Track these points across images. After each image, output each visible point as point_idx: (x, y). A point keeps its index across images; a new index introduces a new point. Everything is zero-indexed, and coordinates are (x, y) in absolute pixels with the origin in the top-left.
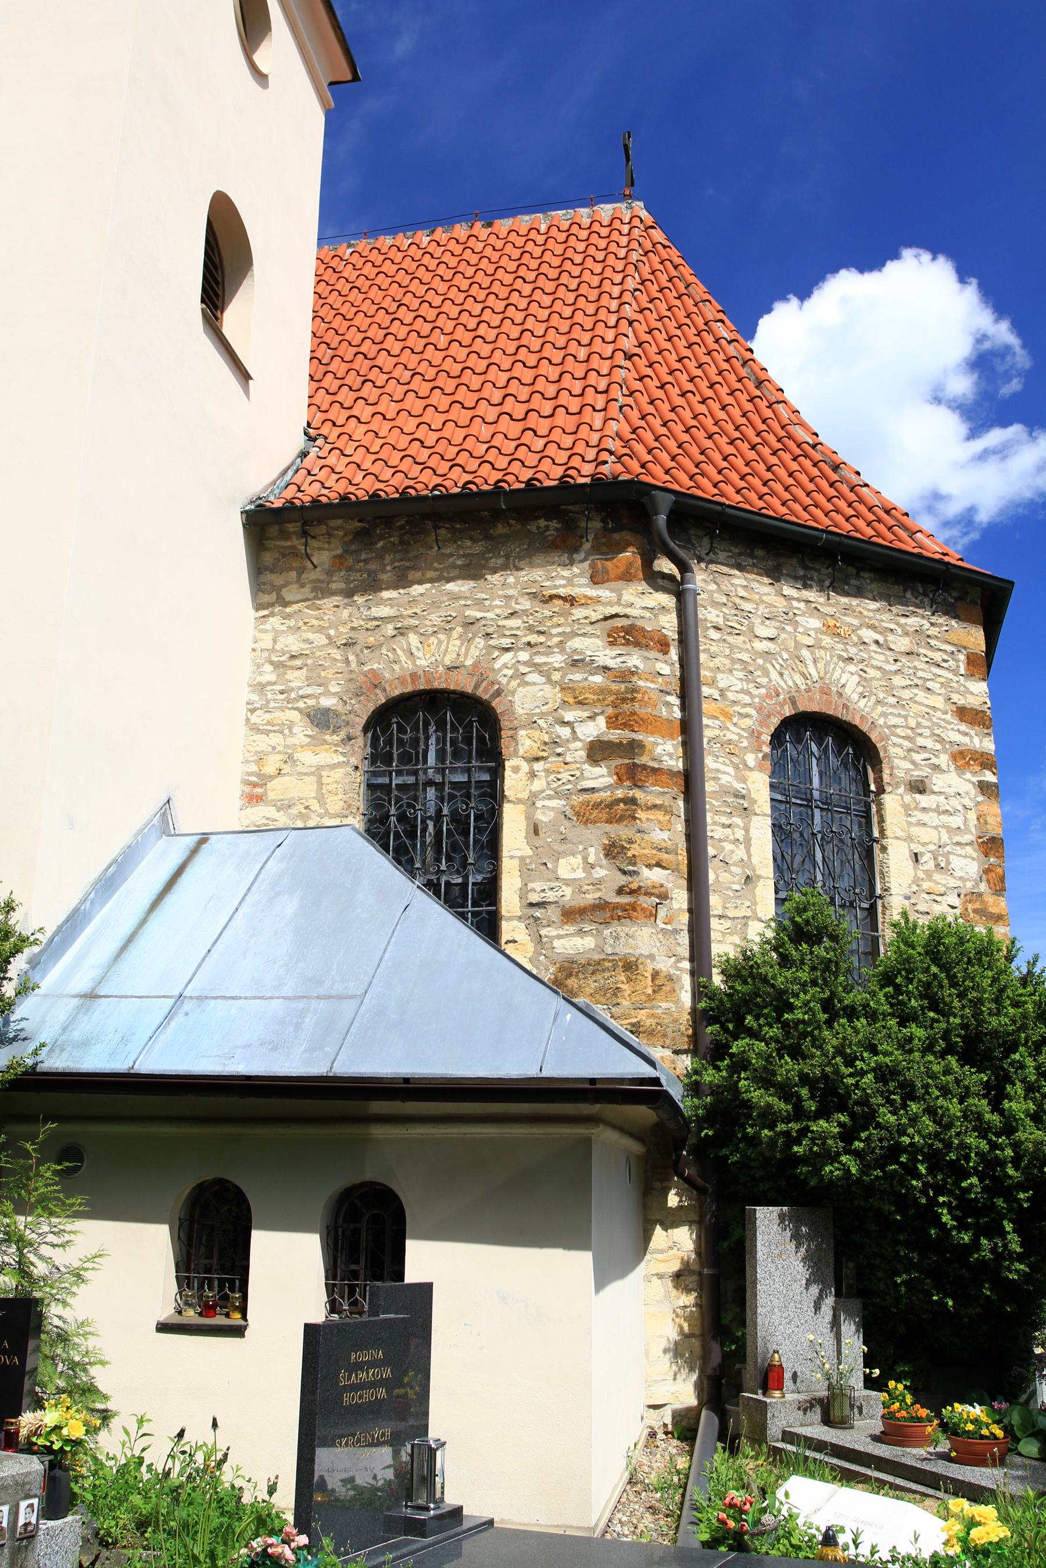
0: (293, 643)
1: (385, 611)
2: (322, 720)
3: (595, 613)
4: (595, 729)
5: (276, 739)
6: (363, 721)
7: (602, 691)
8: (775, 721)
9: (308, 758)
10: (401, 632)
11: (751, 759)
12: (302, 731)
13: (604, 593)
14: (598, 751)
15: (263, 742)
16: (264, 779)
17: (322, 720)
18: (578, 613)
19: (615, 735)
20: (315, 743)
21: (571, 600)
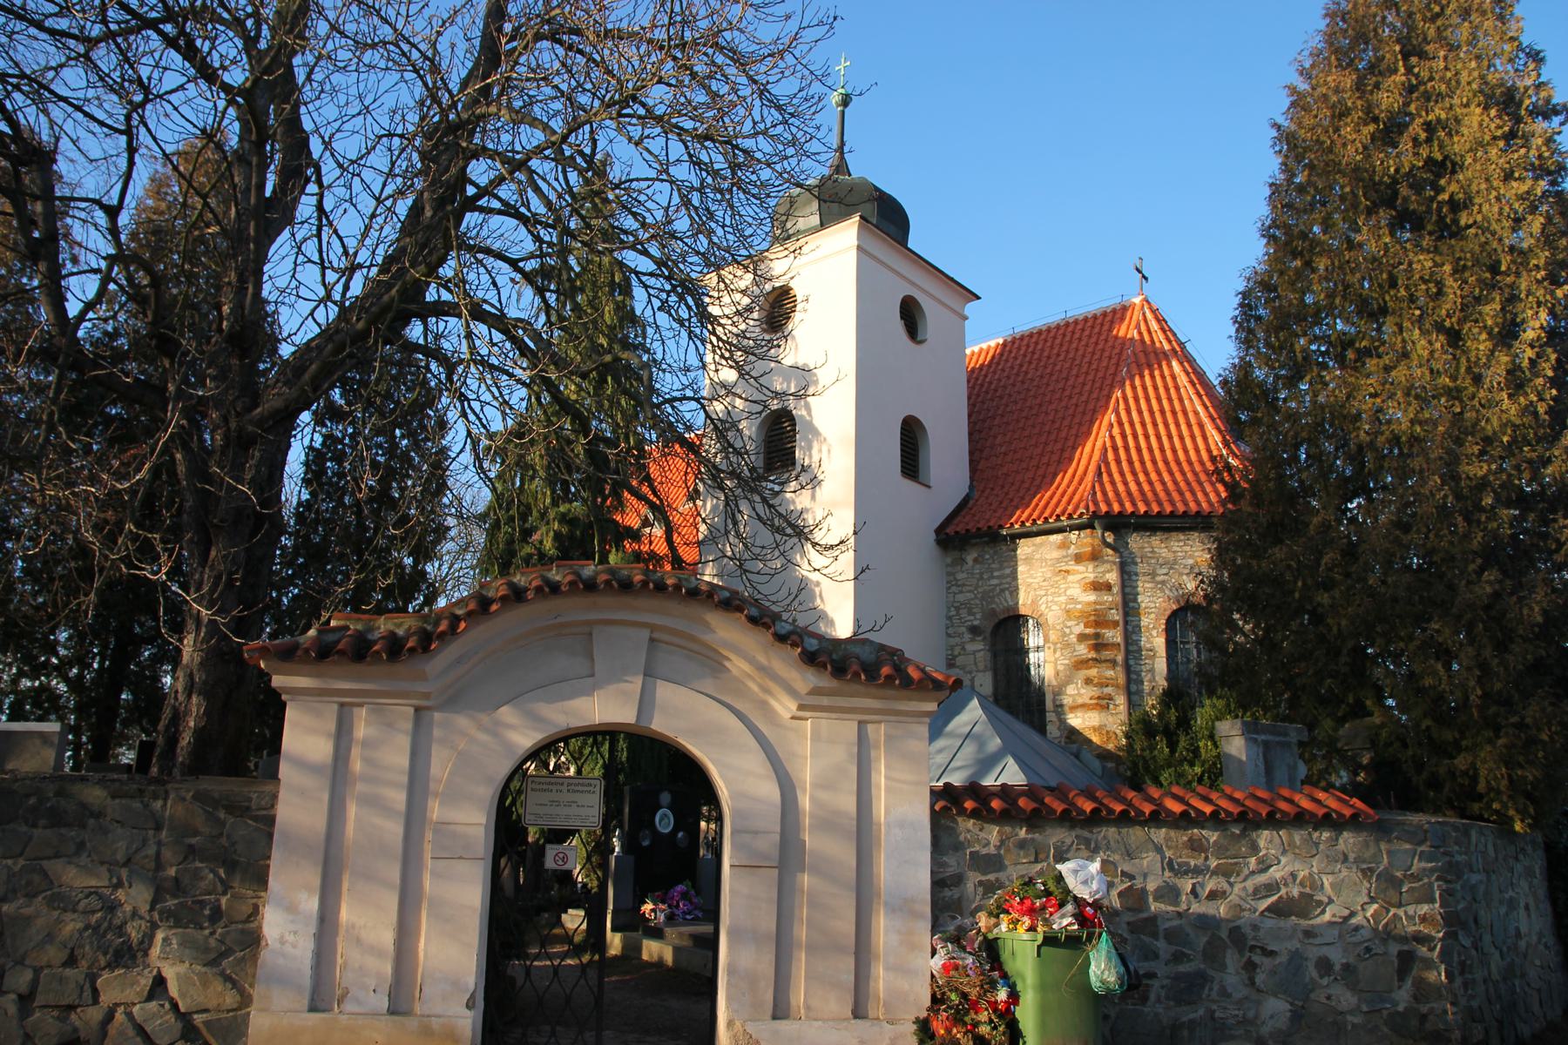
0: (960, 597)
1: (995, 582)
2: (974, 630)
3: (1080, 576)
4: (1080, 629)
5: (957, 640)
6: (989, 630)
7: (1081, 611)
8: (1168, 612)
9: (970, 647)
10: (1002, 591)
11: (1154, 633)
12: (967, 636)
13: (1080, 568)
14: (1082, 637)
15: (953, 641)
16: (955, 657)
17: (974, 630)
18: (1070, 578)
19: (1088, 631)
20: (972, 640)
21: (1067, 572)
